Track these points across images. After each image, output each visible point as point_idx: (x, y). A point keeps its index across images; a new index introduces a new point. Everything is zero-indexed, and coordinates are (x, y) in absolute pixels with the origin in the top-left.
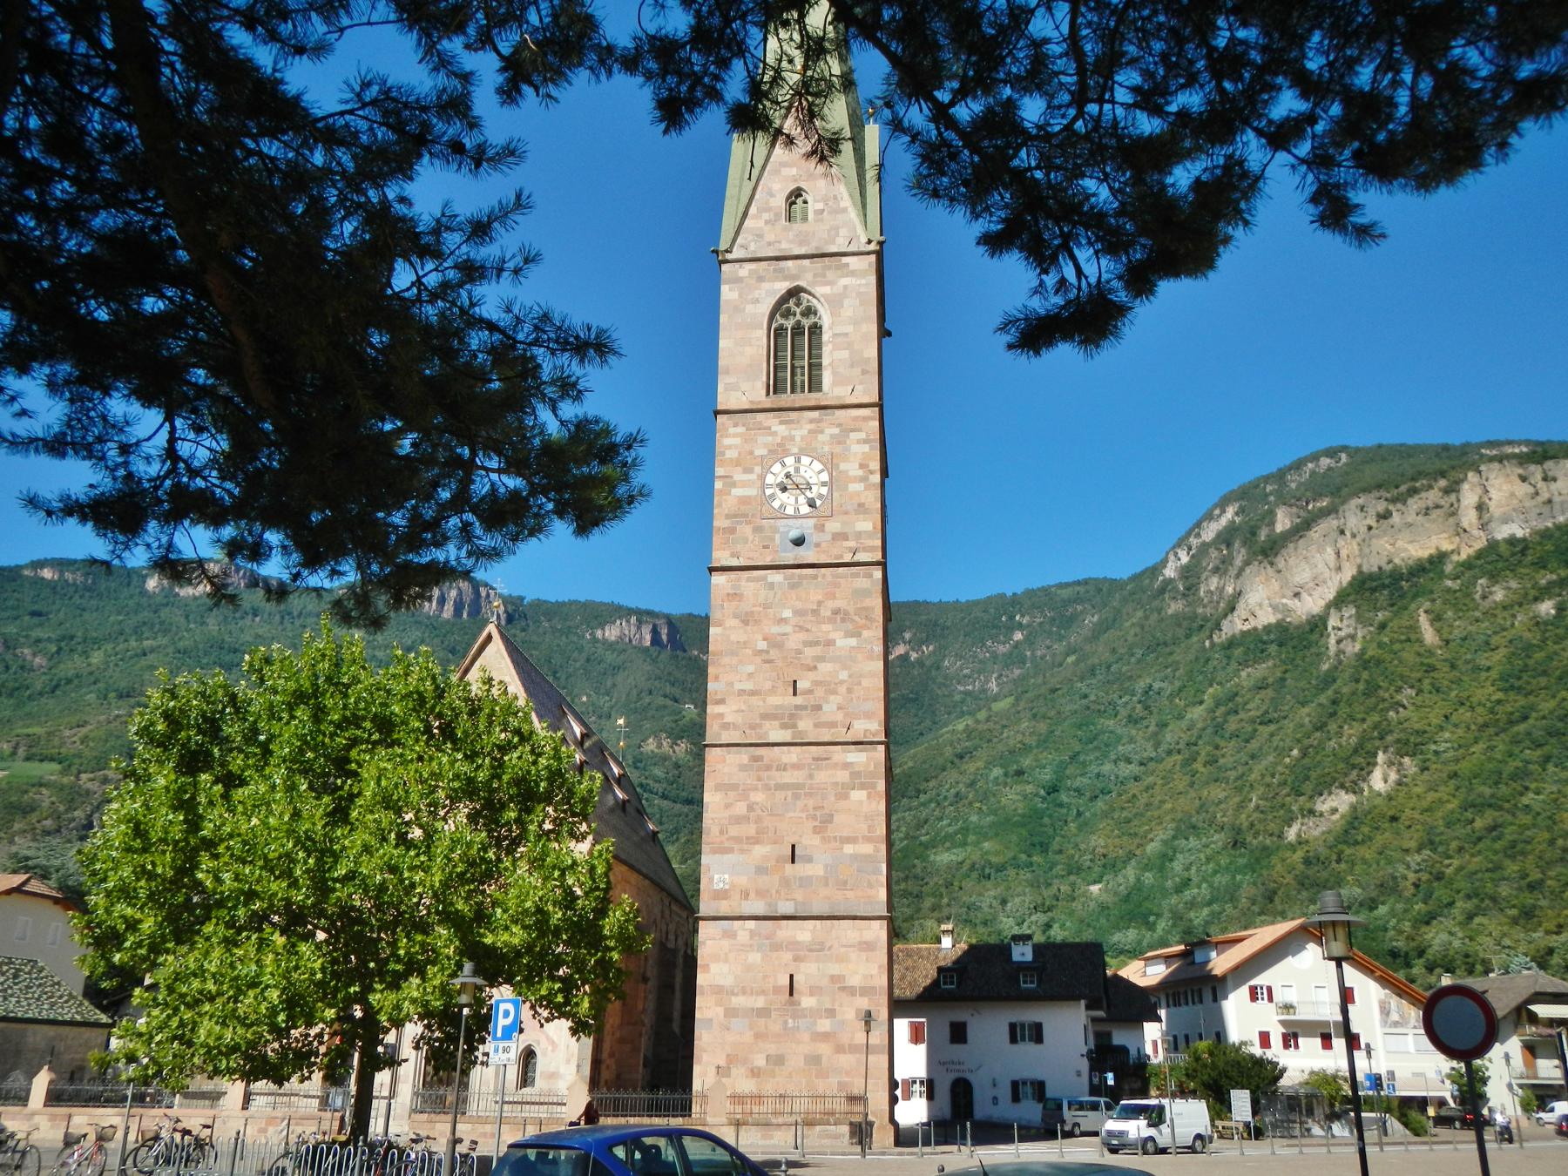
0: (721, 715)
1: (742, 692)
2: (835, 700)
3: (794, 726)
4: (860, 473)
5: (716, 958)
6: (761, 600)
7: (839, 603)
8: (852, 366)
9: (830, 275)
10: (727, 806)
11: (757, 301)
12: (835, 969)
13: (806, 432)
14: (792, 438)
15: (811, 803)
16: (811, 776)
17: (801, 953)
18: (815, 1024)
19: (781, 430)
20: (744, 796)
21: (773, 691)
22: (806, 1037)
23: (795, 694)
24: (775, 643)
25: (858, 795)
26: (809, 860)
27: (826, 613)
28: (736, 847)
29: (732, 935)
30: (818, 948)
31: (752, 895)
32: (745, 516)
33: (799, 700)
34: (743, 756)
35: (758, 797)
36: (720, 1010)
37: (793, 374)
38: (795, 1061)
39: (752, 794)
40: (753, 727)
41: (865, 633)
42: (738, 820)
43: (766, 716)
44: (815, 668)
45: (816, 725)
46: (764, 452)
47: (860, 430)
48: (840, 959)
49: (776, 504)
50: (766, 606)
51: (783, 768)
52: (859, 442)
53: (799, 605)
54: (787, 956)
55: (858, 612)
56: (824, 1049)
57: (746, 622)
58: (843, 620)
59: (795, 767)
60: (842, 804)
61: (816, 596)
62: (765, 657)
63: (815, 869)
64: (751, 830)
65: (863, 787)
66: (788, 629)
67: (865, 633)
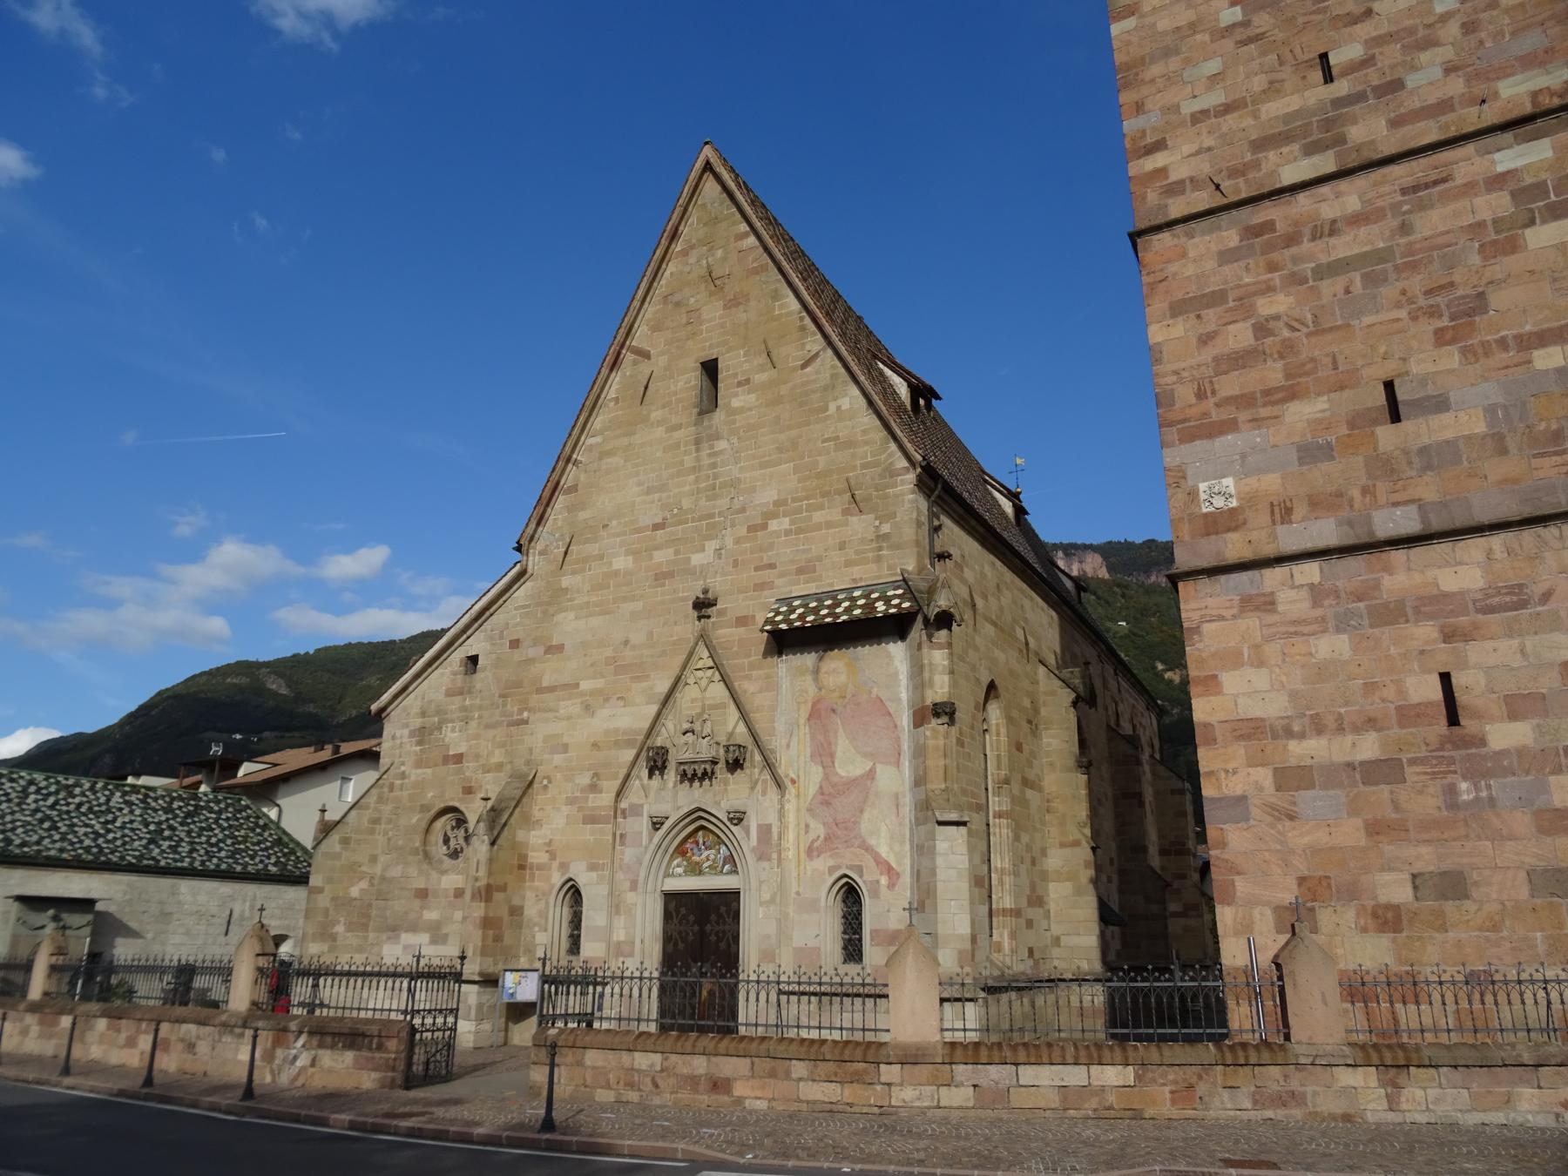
0: (1162, 172)
1: (1198, 117)
2: (1432, 62)
3: (1341, 140)
5: (1233, 660)
10: (1205, 339)
15: (1416, 283)
16: (1405, 228)
20: (1244, 306)
21: (1274, 89)
22: (1522, 821)
23: (1328, 78)
26: (1440, 404)
28: (1243, 416)
30: (1510, 601)
31: (1300, 511)
33: (1341, 87)
34: (1230, 236)
35: (1278, 304)
36: (1264, 776)
42: (1238, 360)
43: (1262, 144)
45: (1395, 124)
51: (1333, 229)
54: (1425, 632)
62: (1241, 34)
64: (1273, 373)
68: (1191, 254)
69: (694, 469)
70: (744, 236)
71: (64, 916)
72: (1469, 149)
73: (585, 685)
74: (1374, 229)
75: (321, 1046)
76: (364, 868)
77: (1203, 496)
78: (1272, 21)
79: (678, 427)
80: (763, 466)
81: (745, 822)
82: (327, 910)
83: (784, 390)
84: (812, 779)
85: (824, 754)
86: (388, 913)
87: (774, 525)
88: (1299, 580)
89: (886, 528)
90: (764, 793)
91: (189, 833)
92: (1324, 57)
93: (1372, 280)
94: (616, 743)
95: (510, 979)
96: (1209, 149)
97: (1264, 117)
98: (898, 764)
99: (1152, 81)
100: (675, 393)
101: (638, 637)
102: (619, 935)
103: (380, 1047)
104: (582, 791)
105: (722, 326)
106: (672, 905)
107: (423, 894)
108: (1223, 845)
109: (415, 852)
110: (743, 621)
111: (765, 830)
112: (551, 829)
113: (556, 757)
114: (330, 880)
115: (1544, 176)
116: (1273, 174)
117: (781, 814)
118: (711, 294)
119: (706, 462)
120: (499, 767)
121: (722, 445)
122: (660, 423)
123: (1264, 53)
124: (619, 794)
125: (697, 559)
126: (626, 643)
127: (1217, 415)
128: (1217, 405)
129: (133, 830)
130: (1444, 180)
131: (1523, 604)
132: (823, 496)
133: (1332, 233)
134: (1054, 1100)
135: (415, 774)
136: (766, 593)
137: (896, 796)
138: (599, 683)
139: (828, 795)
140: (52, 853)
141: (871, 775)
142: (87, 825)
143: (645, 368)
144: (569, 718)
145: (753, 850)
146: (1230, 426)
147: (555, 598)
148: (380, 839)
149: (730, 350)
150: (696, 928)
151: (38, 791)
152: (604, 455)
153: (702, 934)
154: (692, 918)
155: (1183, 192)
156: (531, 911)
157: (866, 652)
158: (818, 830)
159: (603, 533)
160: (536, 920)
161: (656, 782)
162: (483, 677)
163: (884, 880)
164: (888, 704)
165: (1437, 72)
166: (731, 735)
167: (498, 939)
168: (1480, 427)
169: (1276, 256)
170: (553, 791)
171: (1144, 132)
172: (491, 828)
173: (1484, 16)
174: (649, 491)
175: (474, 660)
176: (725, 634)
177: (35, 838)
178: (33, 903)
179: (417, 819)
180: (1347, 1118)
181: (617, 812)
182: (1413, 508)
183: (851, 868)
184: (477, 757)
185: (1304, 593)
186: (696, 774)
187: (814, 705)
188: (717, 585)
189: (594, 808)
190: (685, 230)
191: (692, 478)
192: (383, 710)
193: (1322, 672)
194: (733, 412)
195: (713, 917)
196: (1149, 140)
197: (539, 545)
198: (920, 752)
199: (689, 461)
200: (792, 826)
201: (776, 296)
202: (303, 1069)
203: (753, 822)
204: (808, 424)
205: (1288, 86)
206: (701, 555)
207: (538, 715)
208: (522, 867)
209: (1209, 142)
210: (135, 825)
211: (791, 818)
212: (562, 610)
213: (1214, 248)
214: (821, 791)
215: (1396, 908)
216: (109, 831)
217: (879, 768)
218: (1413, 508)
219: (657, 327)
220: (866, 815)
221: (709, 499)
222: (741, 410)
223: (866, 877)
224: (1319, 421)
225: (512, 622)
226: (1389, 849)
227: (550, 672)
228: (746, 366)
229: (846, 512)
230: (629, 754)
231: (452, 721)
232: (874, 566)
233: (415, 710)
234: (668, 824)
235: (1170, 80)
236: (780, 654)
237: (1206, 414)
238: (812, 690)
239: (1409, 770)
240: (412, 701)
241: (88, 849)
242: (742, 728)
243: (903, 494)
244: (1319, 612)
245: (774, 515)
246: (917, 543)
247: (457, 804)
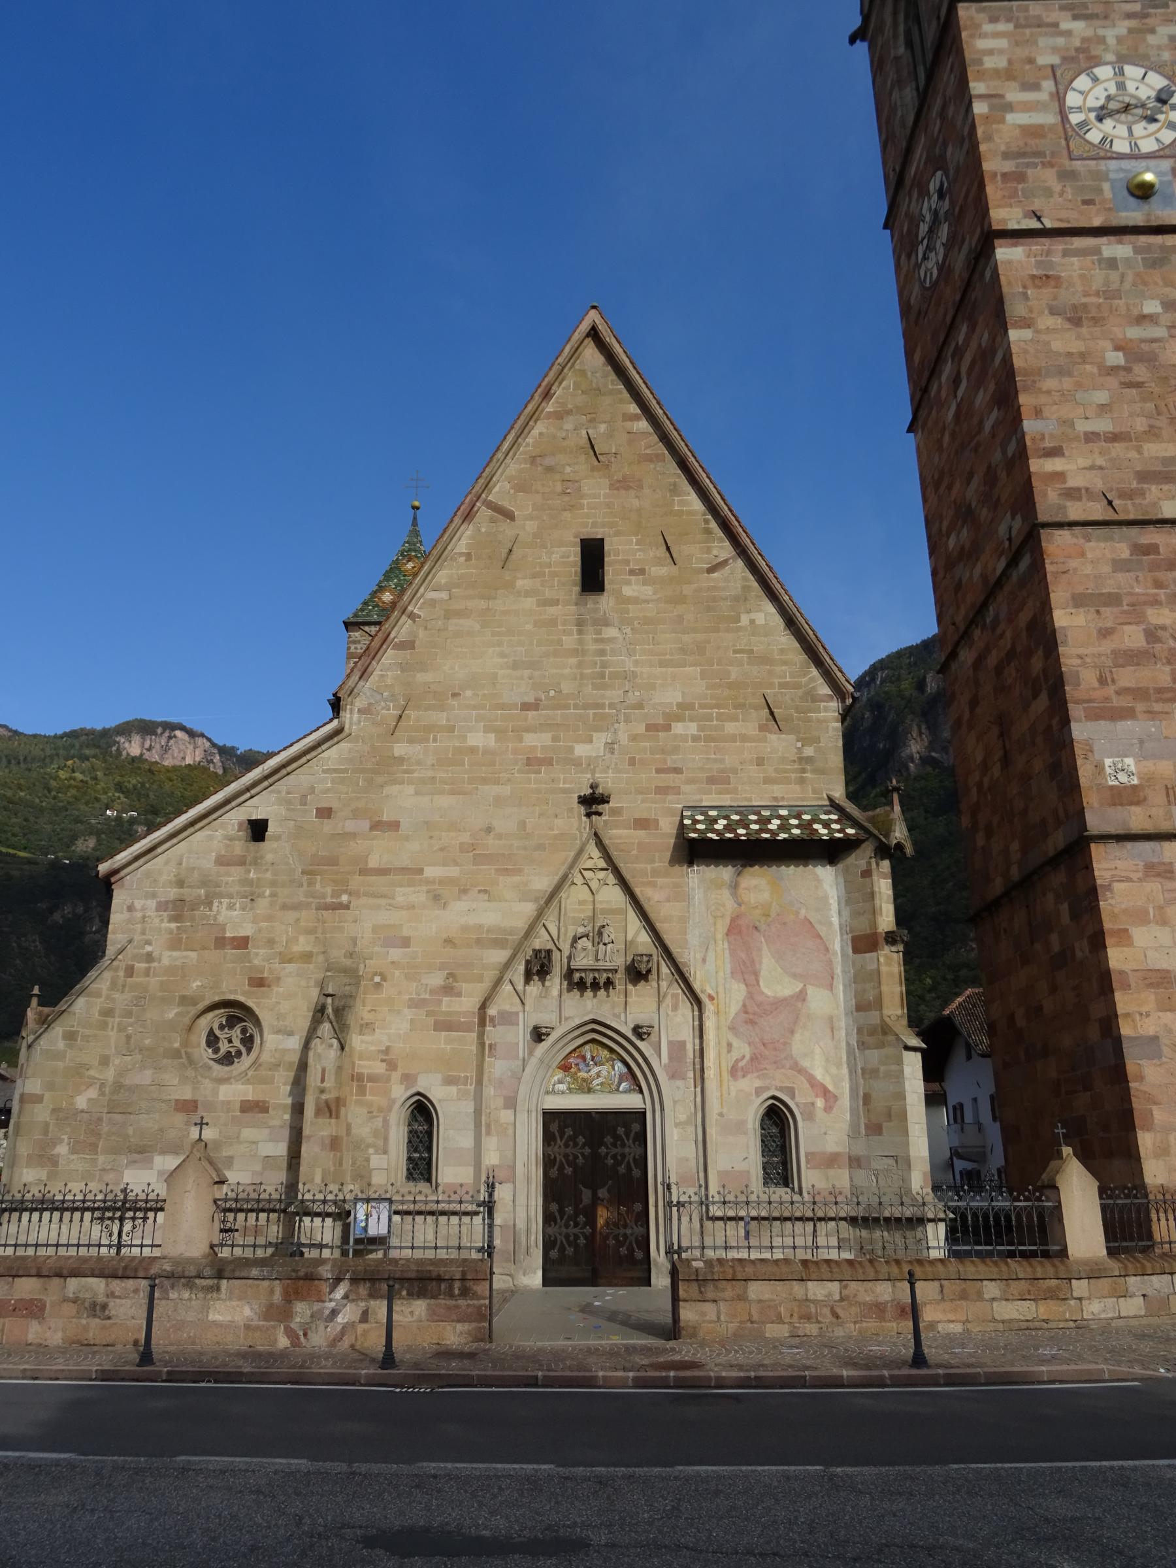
0: (1060, 476)
1: (1091, 437)
5: (1141, 917)
13: (1124, 31)
14: (1102, 40)
20: (1135, 613)
21: (1152, 433)
24: (1134, 353)
28: (1140, 707)
32: (1038, 154)
34: (1119, 546)
42: (1132, 658)
43: (1145, 476)
57: (1076, 322)
68: (1089, 555)
69: (575, 652)
73: (430, 872)
76: (92, 1073)
77: (1108, 771)
78: (1149, 375)
79: (555, 602)
80: (662, 664)
81: (654, 1038)
82: (47, 1124)
83: (688, 590)
85: (747, 971)
86: (130, 1131)
87: (678, 728)
89: (809, 751)
90: (675, 1008)
94: (478, 941)
96: (1101, 468)
97: (1146, 454)
98: (831, 987)
99: (1049, 392)
100: (549, 566)
102: (491, 1158)
104: (432, 992)
105: (608, 506)
106: (554, 1127)
108: (1141, 1078)
109: (176, 1054)
110: (642, 824)
112: (394, 1036)
113: (392, 950)
116: (1155, 505)
118: (593, 469)
119: (592, 647)
120: (307, 957)
121: (611, 632)
122: (527, 594)
123: (1143, 400)
125: (581, 750)
126: (489, 830)
127: (1117, 702)
128: (1118, 693)
132: (736, 707)
135: (168, 958)
136: (670, 797)
137: (831, 1018)
138: (453, 872)
139: (754, 1013)
143: (507, 530)
144: (411, 907)
145: (666, 1068)
146: (1127, 714)
147: (382, 767)
149: (618, 534)
150: (587, 1151)
152: (449, 615)
154: (581, 1140)
155: (1080, 499)
157: (791, 873)
158: (742, 1049)
160: (371, 1140)
161: (534, 988)
163: (820, 1103)
164: (818, 927)
169: (1161, 575)
170: (388, 990)
171: (1043, 438)
174: (515, 666)
176: (618, 835)
183: (781, 1089)
184: (271, 942)
187: (733, 920)
188: (608, 782)
189: (449, 1013)
190: (558, 392)
191: (573, 661)
192: (115, 872)
195: (608, 1139)
197: (359, 703)
199: (569, 641)
200: (712, 1044)
204: (717, 630)
206: (588, 747)
207: (363, 900)
209: (1100, 461)
212: (395, 782)
214: (745, 1009)
217: (811, 990)
219: (522, 487)
220: (797, 1036)
221: (595, 687)
222: (635, 601)
223: (797, 1099)
225: (319, 787)
227: (379, 852)
228: (639, 555)
229: (762, 728)
230: (500, 956)
231: (230, 896)
232: (797, 787)
234: (554, 1036)
236: (691, 863)
238: (730, 904)
240: (163, 866)
243: (825, 721)
245: (680, 719)
247: (241, 999)
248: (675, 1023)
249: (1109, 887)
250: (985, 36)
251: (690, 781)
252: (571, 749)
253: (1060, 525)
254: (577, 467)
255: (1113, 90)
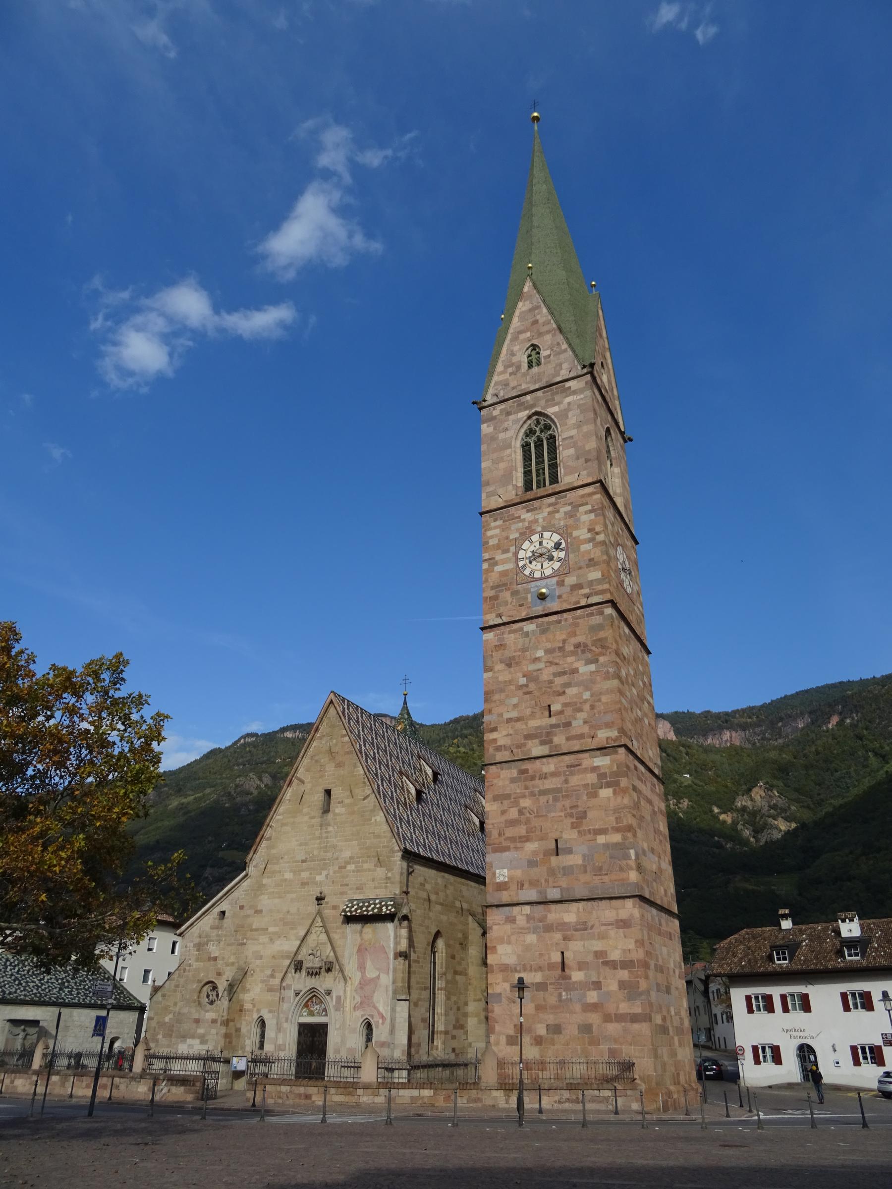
0: (495, 740)
1: (509, 720)
2: (581, 716)
3: (551, 742)
4: (589, 535)
5: (501, 941)
6: (520, 646)
7: (580, 639)
8: (577, 458)
9: (557, 398)
10: (503, 812)
11: (507, 429)
12: (597, 945)
14: (536, 521)
15: (568, 803)
16: (566, 781)
17: (568, 932)
18: (585, 996)
19: (527, 516)
21: (533, 716)
22: (578, 1007)
25: (606, 793)
26: (570, 851)
27: (569, 648)
28: (512, 845)
29: (511, 920)
30: (583, 927)
31: (526, 886)
32: (505, 585)
33: (553, 720)
35: (526, 803)
37: (538, 475)
38: (571, 1030)
39: (521, 801)
40: (519, 747)
41: (602, 659)
42: (512, 823)
43: (528, 737)
44: (564, 692)
45: (568, 739)
46: (517, 535)
47: (587, 504)
48: (602, 937)
49: (527, 572)
50: (524, 650)
51: (544, 777)
52: (586, 513)
53: (549, 645)
54: (558, 936)
55: (594, 643)
56: (594, 1018)
57: (509, 665)
58: (583, 652)
59: (554, 774)
60: (593, 802)
61: (560, 636)
63: (574, 860)
64: (522, 830)
65: (608, 785)
66: (541, 665)
67: (602, 659)
69: (320, 838)
70: (344, 736)
71: (27, 1029)
72: (587, 755)
73: (271, 929)
74: (558, 779)
75: (172, 1085)
80: (346, 840)
83: (356, 808)
84: (357, 977)
85: (362, 967)
87: (349, 867)
88: (524, 912)
89: (389, 875)
91: (76, 983)
92: (549, 706)
93: (556, 799)
95: (235, 1060)
98: (388, 973)
101: (293, 910)
102: (280, 1041)
103: (194, 1085)
107: (197, 1021)
108: (493, 1011)
109: (194, 1001)
110: (335, 907)
111: (339, 998)
112: (254, 993)
114: (156, 1014)
115: (607, 770)
116: (530, 750)
117: (345, 991)
119: (324, 835)
120: (233, 964)
121: (330, 829)
123: (531, 700)
124: (282, 980)
125: (318, 878)
126: (288, 912)
127: (504, 844)
129: (52, 983)
130: (579, 765)
131: (585, 929)
133: (545, 778)
134: (408, 1101)
135: (196, 965)
138: (276, 929)
139: (364, 983)
140: (22, 997)
141: (379, 976)
142: (33, 982)
143: (302, 788)
147: (259, 888)
148: (179, 995)
151: (11, 965)
152: (283, 825)
153: (313, 1040)
156: (244, 1030)
157: (379, 926)
158: (358, 999)
159: (281, 861)
162: (227, 922)
163: (380, 1021)
165: (581, 722)
166: (328, 957)
167: (230, 1042)
168: (580, 862)
169: (527, 783)
172: (229, 994)
173: (597, 704)
174: (301, 845)
175: (223, 913)
176: (328, 912)
177: (14, 990)
178: (15, 1022)
179: (195, 986)
180: (494, 1106)
181: (282, 988)
182: (559, 889)
184: (223, 958)
185: (524, 918)
186: (314, 973)
188: (326, 890)
190: (321, 728)
191: (318, 841)
193: (528, 948)
194: (335, 815)
196: (492, 726)
198: (395, 970)
199: (317, 833)
201: (355, 766)
202: (165, 1094)
203: (334, 995)
204: (364, 825)
205: (537, 716)
207: (251, 941)
208: (241, 1010)
209: (511, 732)
210: (53, 980)
211: (348, 993)
212: (262, 894)
213: (509, 776)
215: (541, 1037)
216: (42, 984)
217: (381, 975)
218: (559, 889)
219: (308, 770)
221: (325, 852)
224: (534, 851)
226: (541, 1015)
229: (376, 866)
230: (287, 962)
233: (196, 934)
234: (301, 994)
235: (502, 702)
237: (500, 843)
238: (359, 939)
239: (549, 987)
241: (35, 994)
242: (332, 954)
244: (528, 925)
245: (349, 863)
246: (401, 882)
248: (338, 989)
249: (491, 928)
250: (490, 529)
251: (351, 889)
252: (315, 878)
253: (492, 764)
254: (324, 759)
255: (538, 546)
